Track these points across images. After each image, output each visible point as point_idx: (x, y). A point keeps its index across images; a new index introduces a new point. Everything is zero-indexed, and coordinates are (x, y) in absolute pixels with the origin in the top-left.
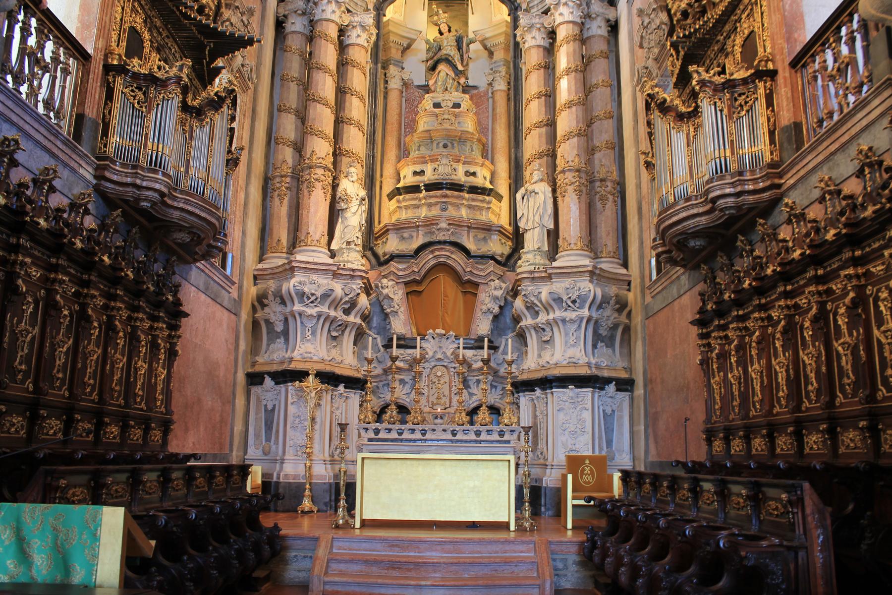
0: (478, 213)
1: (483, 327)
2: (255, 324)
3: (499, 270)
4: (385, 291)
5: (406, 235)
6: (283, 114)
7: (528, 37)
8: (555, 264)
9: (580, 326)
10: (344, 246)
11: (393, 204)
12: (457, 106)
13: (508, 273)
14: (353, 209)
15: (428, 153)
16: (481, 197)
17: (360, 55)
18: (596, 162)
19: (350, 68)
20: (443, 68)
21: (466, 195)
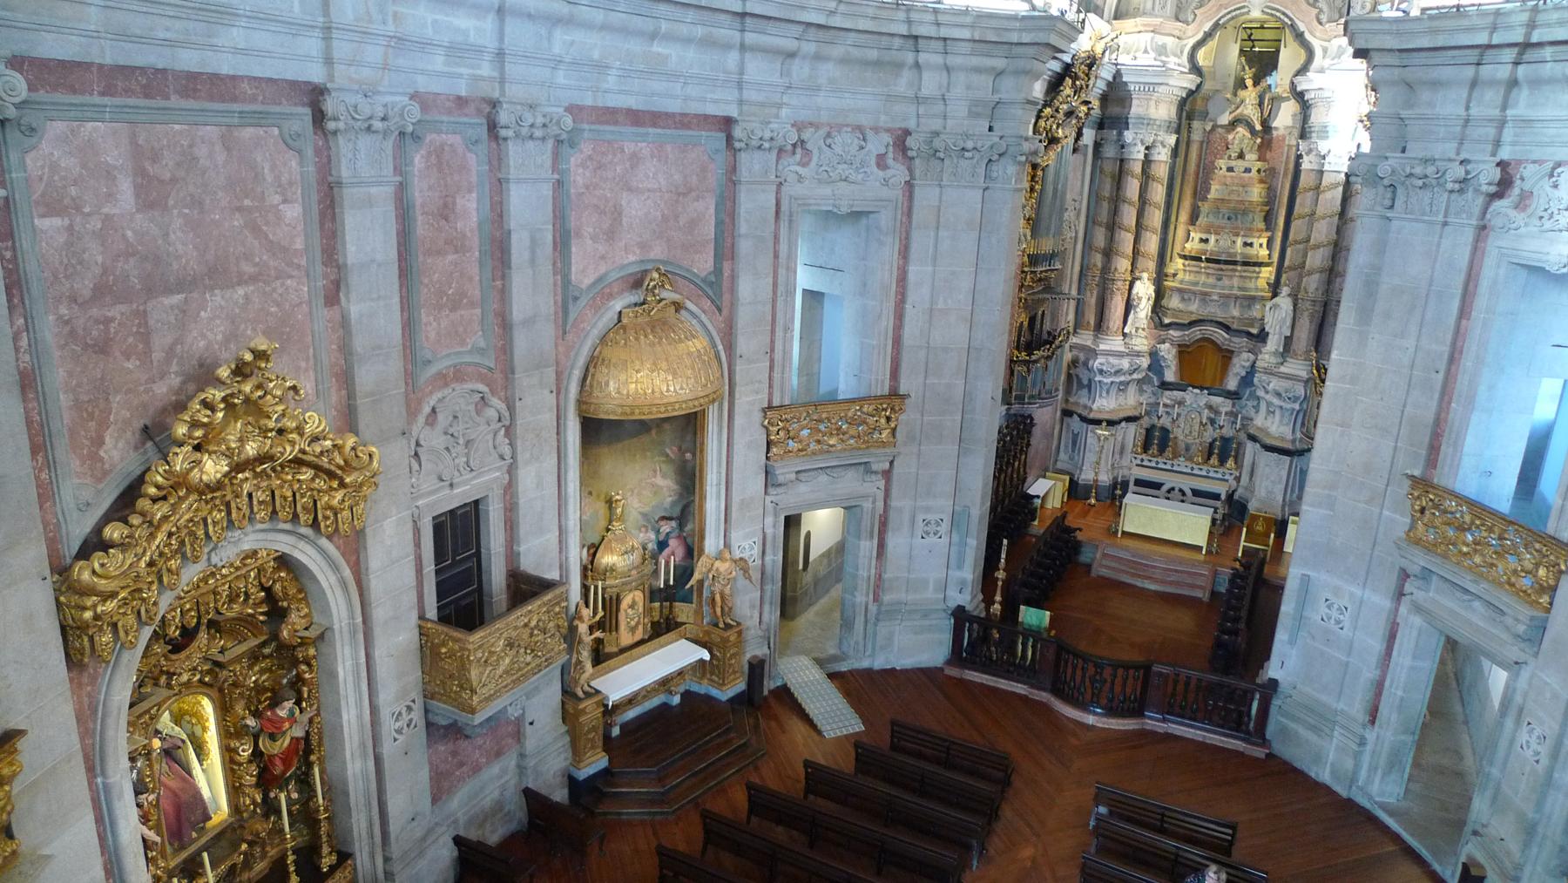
0: (1248, 281)
1: (1232, 384)
2: (1069, 376)
3: (1251, 344)
4: (1162, 354)
5: (1186, 297)
6: (1097, 227)
7: (1305, 158)
8: (1283, 369)
9: (1292, 414)
10: (1133, 331)
11: (1180, 261)
12: (1248, 170)
13: (1259, 344)
14: (1142, 306)
15: (1215, 220)
16: (1251, 268)
17: (1161, 171)
18: (1337, 285)
19: (1150, 181)
20: (1241, 130)
21: (1239, 268)
